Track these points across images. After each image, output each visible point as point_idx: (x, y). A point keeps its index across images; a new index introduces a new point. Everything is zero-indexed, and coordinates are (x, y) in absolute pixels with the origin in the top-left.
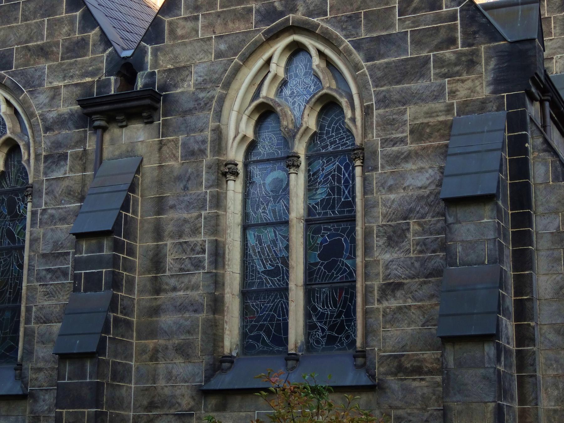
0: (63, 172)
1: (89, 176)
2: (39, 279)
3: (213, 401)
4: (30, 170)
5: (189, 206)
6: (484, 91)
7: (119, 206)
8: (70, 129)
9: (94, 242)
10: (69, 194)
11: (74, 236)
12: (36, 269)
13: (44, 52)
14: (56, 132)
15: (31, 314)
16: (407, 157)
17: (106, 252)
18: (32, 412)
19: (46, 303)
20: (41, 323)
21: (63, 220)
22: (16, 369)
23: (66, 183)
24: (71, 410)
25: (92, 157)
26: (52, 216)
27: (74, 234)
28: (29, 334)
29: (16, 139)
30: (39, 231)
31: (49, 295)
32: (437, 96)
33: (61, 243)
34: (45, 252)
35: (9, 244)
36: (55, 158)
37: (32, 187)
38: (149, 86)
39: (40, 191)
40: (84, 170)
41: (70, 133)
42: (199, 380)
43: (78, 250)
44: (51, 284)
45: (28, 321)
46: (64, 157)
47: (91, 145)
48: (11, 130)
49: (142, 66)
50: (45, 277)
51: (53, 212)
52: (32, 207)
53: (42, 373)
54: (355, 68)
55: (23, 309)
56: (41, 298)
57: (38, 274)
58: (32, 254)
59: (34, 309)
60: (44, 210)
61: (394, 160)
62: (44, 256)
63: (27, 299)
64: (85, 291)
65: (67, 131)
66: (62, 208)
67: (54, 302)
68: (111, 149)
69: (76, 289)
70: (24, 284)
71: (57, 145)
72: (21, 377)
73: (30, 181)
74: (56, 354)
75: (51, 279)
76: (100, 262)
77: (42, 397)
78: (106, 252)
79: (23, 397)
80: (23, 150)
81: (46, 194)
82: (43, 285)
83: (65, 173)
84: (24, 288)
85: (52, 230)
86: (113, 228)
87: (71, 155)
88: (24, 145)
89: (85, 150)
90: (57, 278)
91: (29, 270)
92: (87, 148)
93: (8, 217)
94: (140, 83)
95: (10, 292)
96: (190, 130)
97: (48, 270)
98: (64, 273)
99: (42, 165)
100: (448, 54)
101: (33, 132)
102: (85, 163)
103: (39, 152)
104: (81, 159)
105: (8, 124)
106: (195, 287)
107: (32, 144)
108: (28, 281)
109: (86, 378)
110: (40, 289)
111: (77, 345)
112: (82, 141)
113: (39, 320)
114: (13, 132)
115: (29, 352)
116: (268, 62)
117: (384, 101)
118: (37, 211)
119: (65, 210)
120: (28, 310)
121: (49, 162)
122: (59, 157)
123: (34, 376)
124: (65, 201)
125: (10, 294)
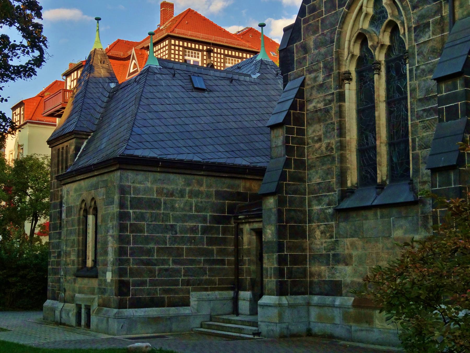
0: (427, 36)
1: (446, 35)
2: (418, 118)
4: (406, 40)
7: (467, 53)
8: (430, 3)
9: (450, 83)
10: (434, 52)
11: (436, 81)
12: (416, 110)
14: (420, 8)
15: (415, 144)
17: (460, 89)
18: (422, 213)
19: (425, 134)
20: (424, 149)
22: (409, 184)
23: (431, 44)
24: (443, 209)
25: (447, 21)
26: (423, 70)
27: (435, 79)
28: (416, 158)
29: (394, 20)
30: (416, 83)
31: (426, 128)
33: (432, 89)
34: (420, 97)
35: (399, 96)
36: (421, 28)
37: (408, 52)
39: (413, 54)
40: (443, 31)
43: (439, 91)
44: (427, 120)
45: (414, 149)
46: (427, 25)
47: (446, 12)
48: (391, 15)
50: (422, 115)
51: (424, 67)
52: (409, 67)
53: (427, 185)
55: (410, 140)
56: (421, 131)
57: (417, 114)
58: (412, 100)
59: (417, 140)
60: (417, 67)
62: (420, 100)
63: (412, 133)
64: (447, 120)
65: (428, 6)
66: (429, 63)
67: (431, 133)
68: (460, 11)
69: (441, 120)
70: (410, 123)
71: (422, 17)
72: (413, 190)
73: (407, 48)
74: (429, 169)
75: (427, 116)
76: (455, 97)
77: (428, 202)
78: (460, 89)
79: (415, 203)
80: (400, 27)
81: (418, 55)
82: (421, 121)
83: (430, 37)
84: (410, 125)
85: (424, 80)
86: (463, 69)
87: (432, 23)
88: (401, 23)
89: (442, 16)
90: (431, 115)
91: (411, 112)
92: (443, 15)
93: (397, 78)
95: (403, 130)
97: (424, 110)
99: (413, 35)
101: (405, 12)
102: (443, 26)
103: (410, 25)
104: (440, 24)
105: (389, 11)
107: (405, 22)
108: (412, 120)
109: (451, 185)
110: (420, 125)
111: (442, 162)
112: (439, 10)
113: (421, 147)
114: (393, 15)
115: (416, 171)
118: (412, 69)
119: (432, 64)
120: (414, 140)
121: (418, 31)
122: (424, 26)
123: (421, 187)
124: (431, 57)
125: (403, 132)
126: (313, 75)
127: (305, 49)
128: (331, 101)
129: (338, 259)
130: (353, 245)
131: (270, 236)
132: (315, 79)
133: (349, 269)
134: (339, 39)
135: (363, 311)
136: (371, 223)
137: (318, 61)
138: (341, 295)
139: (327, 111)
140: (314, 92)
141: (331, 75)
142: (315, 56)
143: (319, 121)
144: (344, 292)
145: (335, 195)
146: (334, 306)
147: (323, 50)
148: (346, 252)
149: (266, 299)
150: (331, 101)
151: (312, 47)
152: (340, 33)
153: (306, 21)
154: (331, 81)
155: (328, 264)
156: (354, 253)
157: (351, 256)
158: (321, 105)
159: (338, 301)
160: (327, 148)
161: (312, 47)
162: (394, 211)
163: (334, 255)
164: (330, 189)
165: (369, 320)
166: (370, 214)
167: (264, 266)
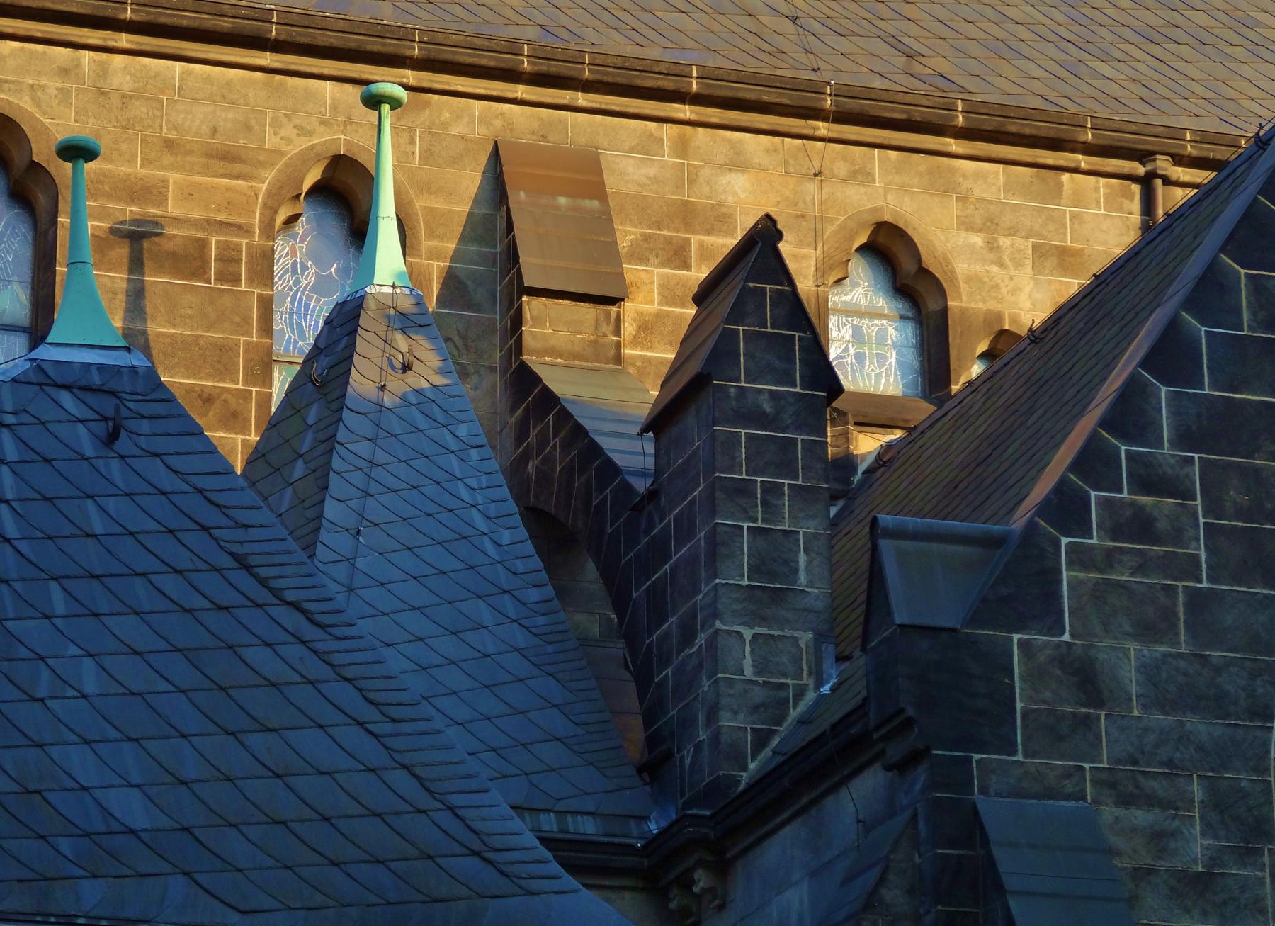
126: (1141, 817)
127: (1087, 680)
132: (1159, 839)
141: (1259, 852)
142: (1151, 738)
147: (1202, 727)
151: (1134, 689)
153: (1080, 558)
154: (1261, 882)
161: (1134, 689)
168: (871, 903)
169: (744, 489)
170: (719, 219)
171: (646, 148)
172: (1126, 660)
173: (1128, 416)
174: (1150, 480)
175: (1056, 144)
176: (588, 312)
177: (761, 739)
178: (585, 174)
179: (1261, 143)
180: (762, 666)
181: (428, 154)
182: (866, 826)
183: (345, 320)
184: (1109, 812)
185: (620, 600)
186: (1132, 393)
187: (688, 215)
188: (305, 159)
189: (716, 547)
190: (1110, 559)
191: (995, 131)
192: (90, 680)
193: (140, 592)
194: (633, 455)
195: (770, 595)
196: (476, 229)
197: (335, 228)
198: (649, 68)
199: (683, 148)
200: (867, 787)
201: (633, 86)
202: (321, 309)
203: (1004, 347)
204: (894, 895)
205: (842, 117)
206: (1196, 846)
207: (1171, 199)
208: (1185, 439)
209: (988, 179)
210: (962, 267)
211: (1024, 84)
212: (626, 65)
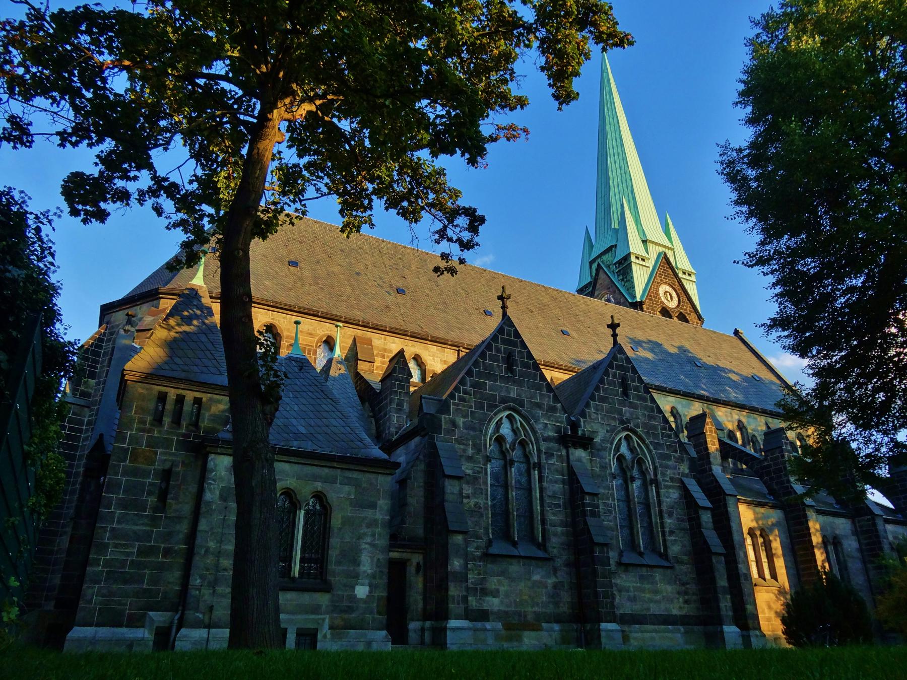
3: (623, 568)
5: (604, 488)
6: (687, 471)
13: (539, 406)
16: (670, 487)
21: (556, 482)
32: (675, 468)
38: (584, 434)
41: (556, 446)
42: (617, 558)
49: (580, 426)
54: (650, 451)
61: (667, 487)
94: (580, 433)
96: (601, 458)
98: (559, 506)
100: (676, 455)
106: (610, 521)
116: (620, 439)
117: (661, 465)
126: (462, 447)
127: (454, 424)
128: (479, 472)
129: (485, 592)
130: (500, 583)
131: (458, 568)
132: (464, 451)
133: (496, 601)
134: (486, 432)
135: (513, 633)
136: (515, 568)
137: (468, 439)
138: (488, 621)
139: (476, 478)
140: (463, 460)
143: (468, 483)
144: (491, 618)
145: (482, 543)
146: (486, 630)
147: (472, 433)
148: (494, 587)
149: (453, 623)
150: (479, 472)
152: (487, 428)
153: (454, 404)
155: (475, 595)
156: (502, 589)
157: (498, 591)
158: (469, 472)
159: (488, 626)
160: (475, 505)
162: (533, 562)
163: (481, 589)
164: (478, 537)
165: (519, 639)
166: (514, 561)
167: (450, 593)
168: (417, 458)
169: (396, 392)
170: (391, 351)
171: (379, 339)
172: (460, 421)
173: (463, 382)
174: (465, 392)
175: (444, 344)
176: (369, 364)
177: (397, 433)
178: (369, 342)
179: (483, 342)
180: (398, 421)
181: (343, 337)
182: (416, 446)
183: (330, 361)
184: (457, 446)
185: (373, 410)
186: (463, 378)
187: (385, 350)
188: (324, 335)
189: (392, 401)
190: (458, 405)
191: (435, 341)
192: (296, 408)
193: (305, 395)
194: (378, 387)
195: (399, 410)
196: (351, 349)
197: (327, 348)
198: (381, 326)
199: (385, 339)
200: (417, 439)
201: (377, 328)
202: (324, 362)
203: (435, 375)
204: (421, 457)
205: (411, 336)
206: (470, 452)
207: (462, 354)
208: (471, 386)
209: (433, 348)
210: (429, 362)
211: (441, 334)
212: (377, 325)
